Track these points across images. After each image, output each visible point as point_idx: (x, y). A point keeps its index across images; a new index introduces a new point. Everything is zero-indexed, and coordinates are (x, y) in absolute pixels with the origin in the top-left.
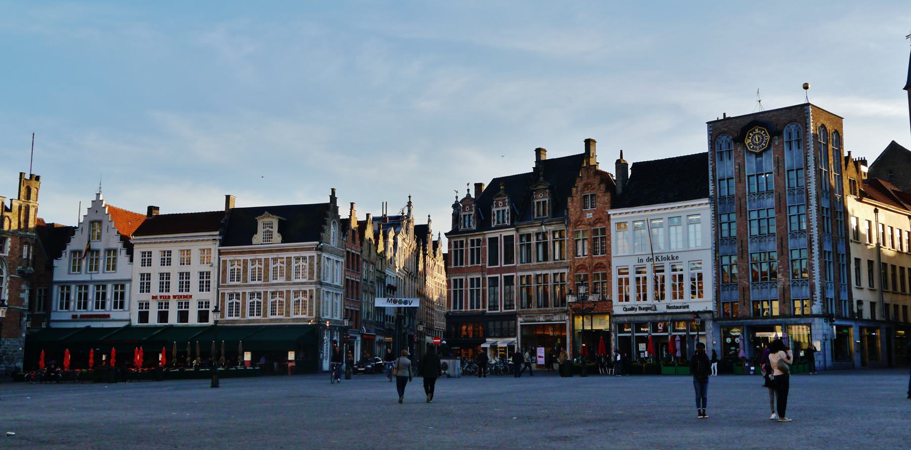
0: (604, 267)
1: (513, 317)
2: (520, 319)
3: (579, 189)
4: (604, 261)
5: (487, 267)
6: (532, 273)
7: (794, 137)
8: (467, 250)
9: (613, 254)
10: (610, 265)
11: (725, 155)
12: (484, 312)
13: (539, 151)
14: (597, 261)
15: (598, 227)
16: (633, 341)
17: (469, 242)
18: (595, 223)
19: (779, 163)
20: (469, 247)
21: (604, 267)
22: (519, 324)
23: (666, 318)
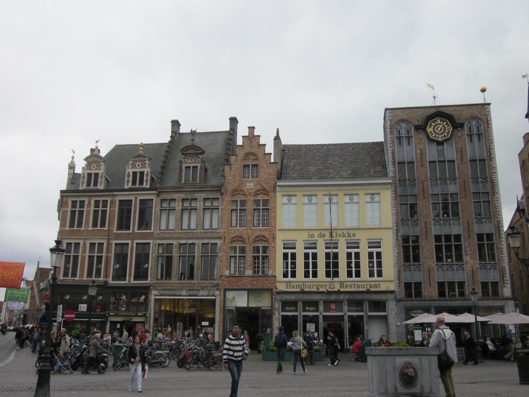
0: (266, 241)
1: (146, 290)
2: (154, 292)
3: (239, 158)
4: (266, 234)
5: (115, 231)
6: (175, 242)
7: (475, 130)
8: (88, 212)
9: (278, 227)
10: (274, 238)
11: (405, 141)
12: (106, 283)
13: (176, 124)
14: (257, 233)
15: (260, 197)
16: (300, 321)
17: (93, 202)
18: (256, 195)
19: (461, 152)
20: (92, 208)
21: (266, 241)
22: (152, 298)
23: (342, 297)
